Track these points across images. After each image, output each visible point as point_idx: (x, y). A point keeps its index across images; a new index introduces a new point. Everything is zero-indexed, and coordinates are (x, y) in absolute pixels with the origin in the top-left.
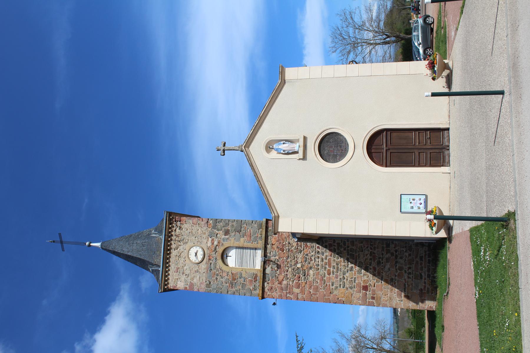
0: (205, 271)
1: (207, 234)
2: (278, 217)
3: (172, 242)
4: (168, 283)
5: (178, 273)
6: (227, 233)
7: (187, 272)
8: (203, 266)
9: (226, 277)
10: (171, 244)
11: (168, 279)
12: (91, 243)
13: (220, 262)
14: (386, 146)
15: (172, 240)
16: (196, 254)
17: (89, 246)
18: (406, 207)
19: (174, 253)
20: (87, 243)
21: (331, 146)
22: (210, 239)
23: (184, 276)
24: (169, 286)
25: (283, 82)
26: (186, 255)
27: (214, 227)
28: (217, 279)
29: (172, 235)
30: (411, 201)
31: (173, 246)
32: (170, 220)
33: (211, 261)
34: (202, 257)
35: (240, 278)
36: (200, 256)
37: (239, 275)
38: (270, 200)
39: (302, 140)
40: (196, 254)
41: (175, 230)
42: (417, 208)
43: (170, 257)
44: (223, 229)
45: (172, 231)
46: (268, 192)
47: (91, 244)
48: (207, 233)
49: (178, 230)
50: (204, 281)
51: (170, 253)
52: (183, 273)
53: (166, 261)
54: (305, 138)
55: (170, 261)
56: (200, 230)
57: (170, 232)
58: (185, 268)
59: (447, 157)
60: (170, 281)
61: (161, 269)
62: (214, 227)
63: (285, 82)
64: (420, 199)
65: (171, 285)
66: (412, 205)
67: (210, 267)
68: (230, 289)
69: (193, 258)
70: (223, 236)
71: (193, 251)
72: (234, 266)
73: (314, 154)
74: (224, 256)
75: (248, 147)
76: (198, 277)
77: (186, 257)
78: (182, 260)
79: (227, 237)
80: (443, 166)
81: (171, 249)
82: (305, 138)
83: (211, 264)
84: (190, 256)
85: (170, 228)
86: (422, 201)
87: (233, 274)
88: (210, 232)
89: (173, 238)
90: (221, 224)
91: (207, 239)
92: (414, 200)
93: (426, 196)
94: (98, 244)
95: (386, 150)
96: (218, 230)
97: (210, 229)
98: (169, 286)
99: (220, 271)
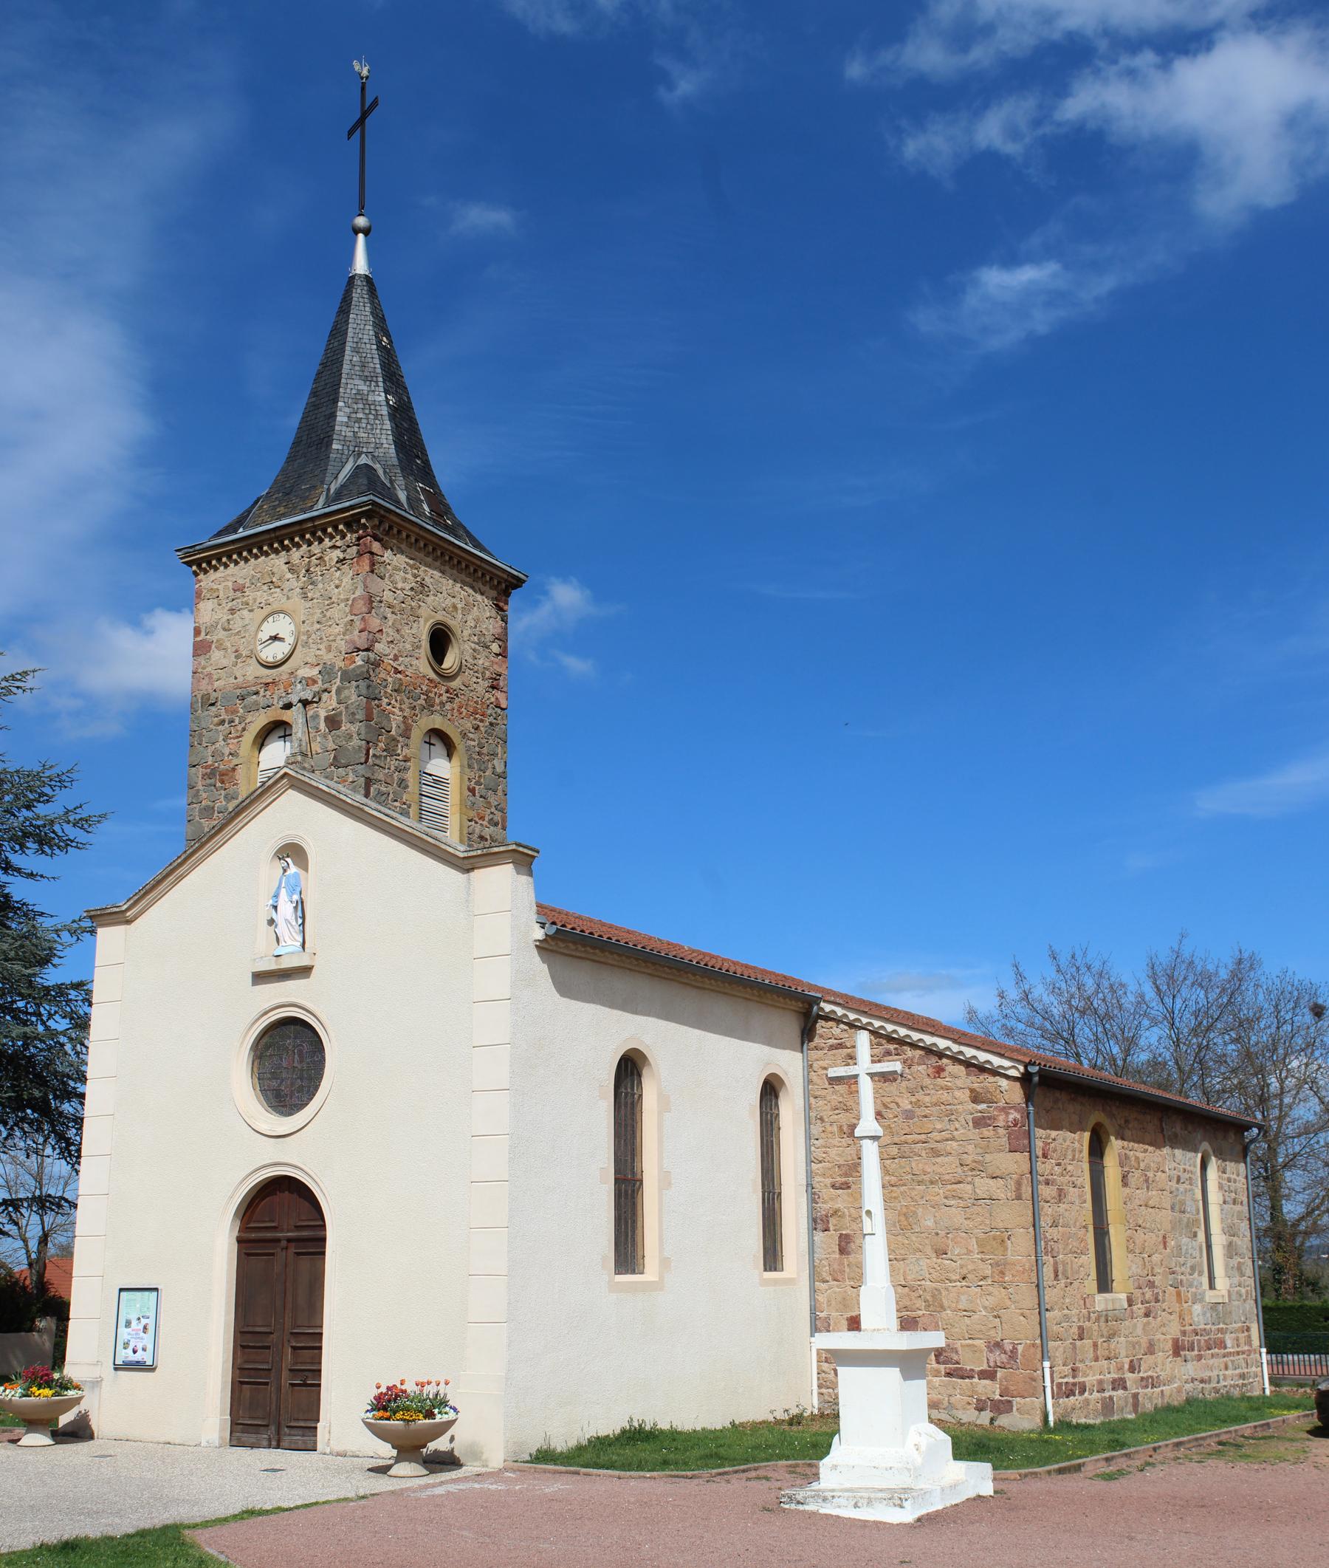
0: (240, 679)
1: (328, 658)
2: (129, 922)
3: (305, 546)
4: (206, 572)
5: (231, 594)
6: (333, 722)
7: (237, 625)
8: (252, 671)
9: (227, 751)
10: (298, 546)
11: (216, 569)
12: (366, 232)
13: (259, 721)
14: (289, 1240)
15: (310, 544)
16: (275, 638)
17: (356, 231)
18: (136, 1306)
19: (277, 562)
20: (361, 221)
21: (290, 1060)
22: (315, 672)
23: (226, 618)
24: (201, 576)
25: (466, 865)
26: (275, 606)
27: (347, 677)
28: (222, 722)
29: (321, 540)
30: (144, 1321)
31: (295, 555)
32: (356, 518)
33: (262, 693)
34: (270, 659)
35: (226, 797)
36: (273, 652)
37: (232, 789)
38: (161, 887)
39: (302, 961)
40: (275, 638)
41: (334, 547)
42: (126, 1337)
43: (267, 554)
44: (342, 707)
45: (332, 537)
46: (182, 877)
47: (361, 236)
48: (331, 655)
49: (337, 554)
50: (216, 684)
51: (277, 552)
52: (232, 611)
53: (254, 545)
54: (305, 971)
55: (256, 557)
56: (337, 629)
57: (324, 531)
58: (245, 612)
59: (251, 1438)
60: (212, 575)
61: (242, 533)
62: (347, 677)
63: (468, 871)
64: (144, 1350)
65: (210, 580)
66: (134, 1323)
67: (249, 694)
68: (200, 771)
69: (269, 629)
70: (323, 714)
71: (282, 626)
72: (262, 767)
73: (267, 1006)
74: (277, 728)
75: (292, 787)
76: (225, 662)
77: (267, 610)
78: (261, 595)
79: (322, 726)
80: (234, 1423)
81: (287, 549)
82: (305, 971)
83: (257, 693)
84: (270, 619)
85: (335, 528)
86: (139, 1356)
87: (234, 769)
88: (333, 665)
89: (316, 548)
90: (354, 698)
91: (314, 661)
92: (145, 1328)
93: (152, 1369)
94: (361, 265)
95: (278, 1240)
96: (339, 691)
97: (342, 664)
98: (201, 576)
99: (240, 728)
